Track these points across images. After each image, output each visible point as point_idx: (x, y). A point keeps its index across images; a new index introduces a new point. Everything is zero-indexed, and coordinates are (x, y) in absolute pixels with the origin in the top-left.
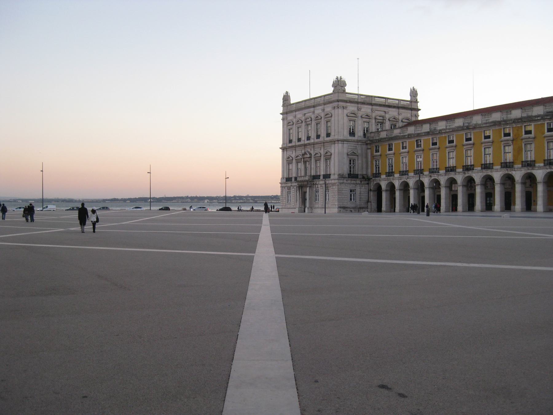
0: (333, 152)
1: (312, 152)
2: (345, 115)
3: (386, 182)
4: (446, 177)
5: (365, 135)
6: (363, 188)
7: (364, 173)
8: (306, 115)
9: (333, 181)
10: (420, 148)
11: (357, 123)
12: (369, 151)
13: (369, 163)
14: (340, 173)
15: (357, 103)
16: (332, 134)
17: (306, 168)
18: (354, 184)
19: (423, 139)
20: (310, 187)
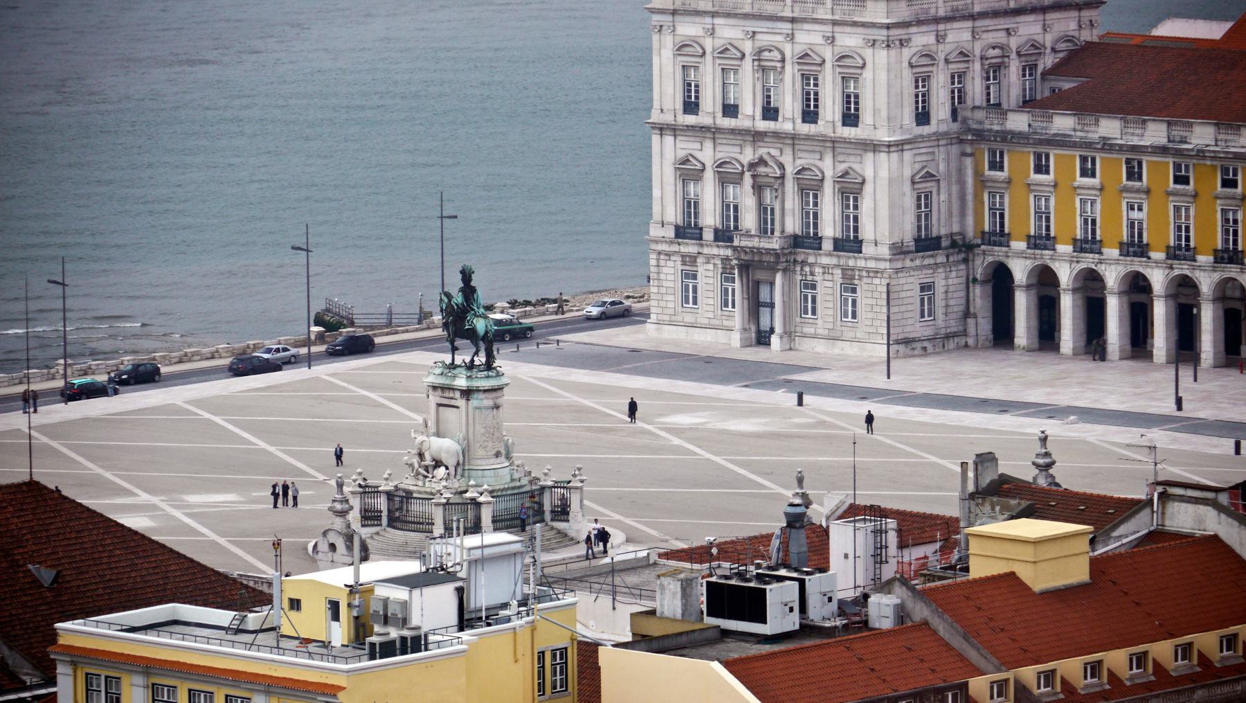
0: (868, 173)
1: (787, 159)
2: (906, 64)
3: (1029, 264)
4: (1216, 276)
5: (954, 113)
6: (954, 274)
7: (956, 229)
8: (758, 37)
9: (872, 264)
10: (1137, 184)
11: (934, 82)
12: (968, 162)
13: (970, 198)
14: (896, 239)
15: (937, 20)
16: (866, 117)
17: (762, 209)
18: (928, 266)
19: (1145, 159)
20: (785, 270)
